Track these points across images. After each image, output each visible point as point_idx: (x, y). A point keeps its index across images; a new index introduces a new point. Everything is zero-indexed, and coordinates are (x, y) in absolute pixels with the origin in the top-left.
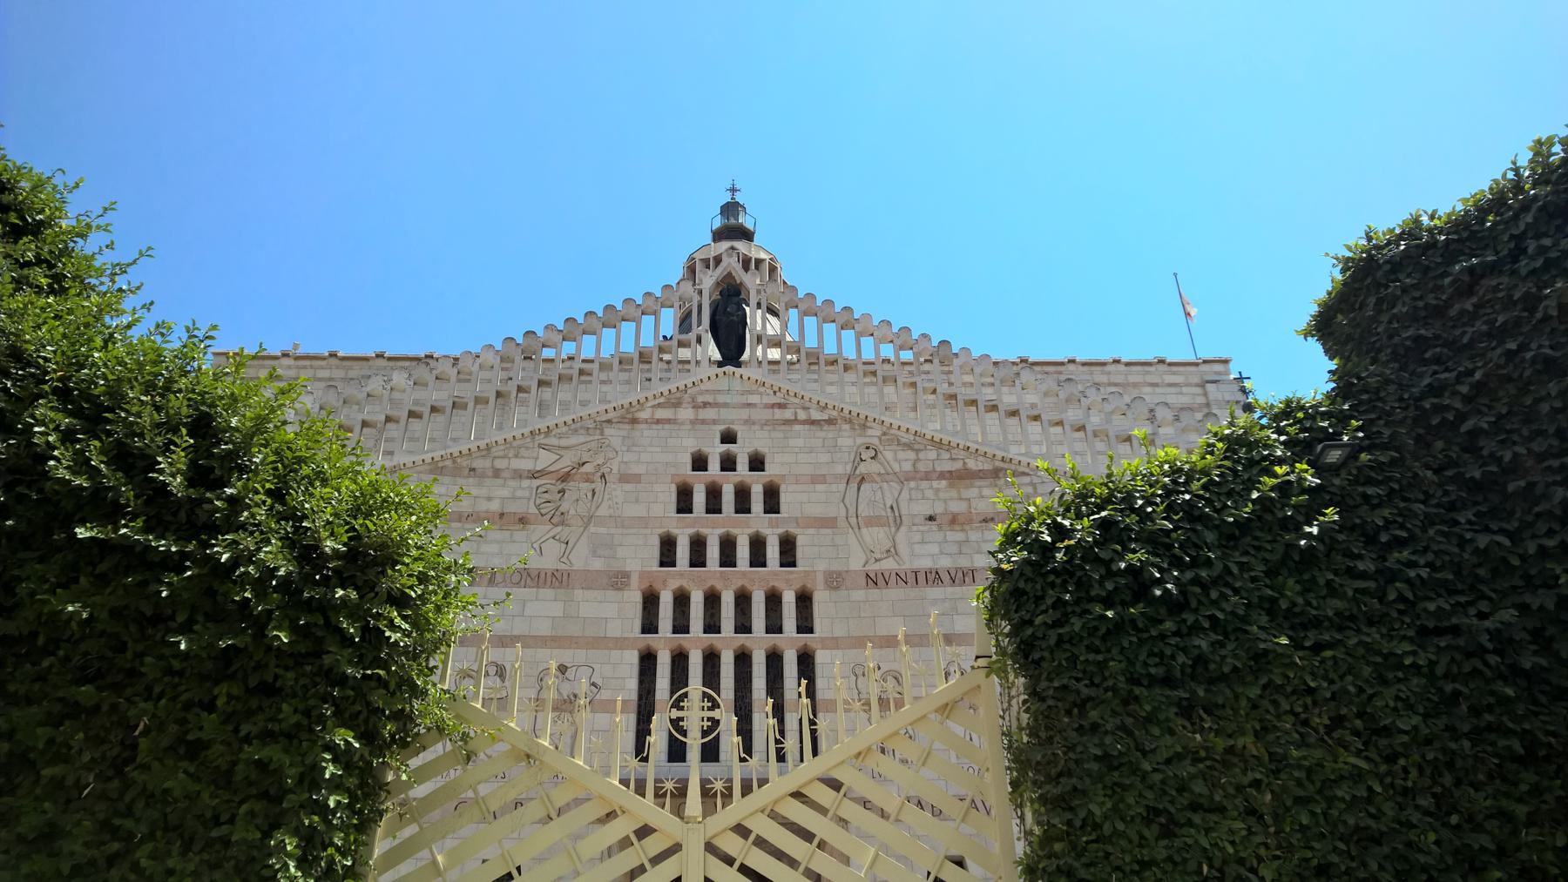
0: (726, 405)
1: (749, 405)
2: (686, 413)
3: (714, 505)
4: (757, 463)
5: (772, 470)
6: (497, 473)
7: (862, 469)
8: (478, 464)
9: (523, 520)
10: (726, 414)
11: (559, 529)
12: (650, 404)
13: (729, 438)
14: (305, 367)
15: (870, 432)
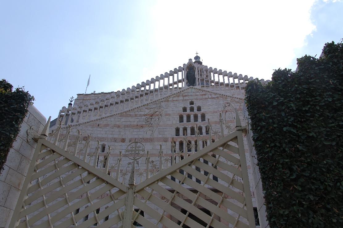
0: (191, 95)
1: (196, 95)
2: (181, 98)
3: (189, 120)
4: (199, 109)
5: (203, 111)
6: (136, 115)
7: (226, 109)
8: (131, 114)
9: (142, 127)
10: (191, 98)
11: (150, 128)
12: (172, 96)
13: (192, 103)
14: (96, 96)
15: (227, 99)
